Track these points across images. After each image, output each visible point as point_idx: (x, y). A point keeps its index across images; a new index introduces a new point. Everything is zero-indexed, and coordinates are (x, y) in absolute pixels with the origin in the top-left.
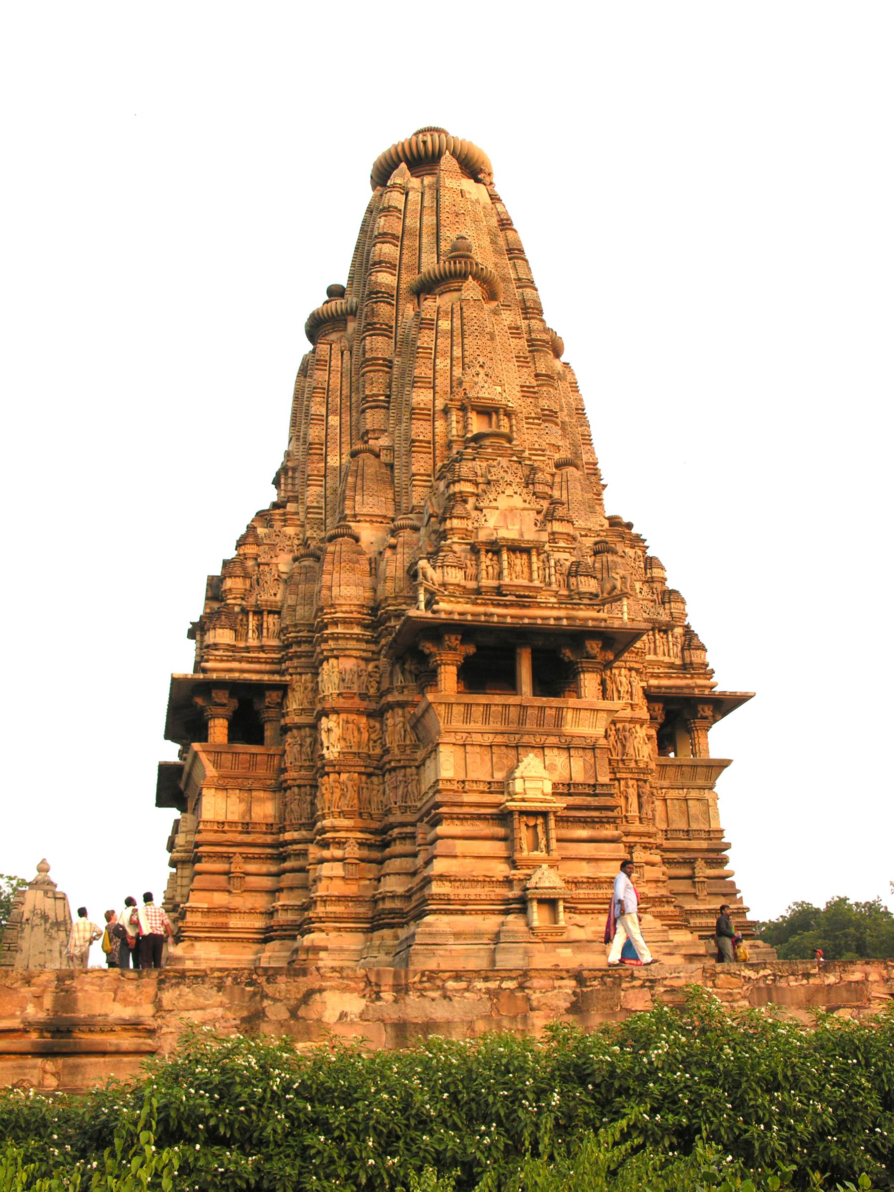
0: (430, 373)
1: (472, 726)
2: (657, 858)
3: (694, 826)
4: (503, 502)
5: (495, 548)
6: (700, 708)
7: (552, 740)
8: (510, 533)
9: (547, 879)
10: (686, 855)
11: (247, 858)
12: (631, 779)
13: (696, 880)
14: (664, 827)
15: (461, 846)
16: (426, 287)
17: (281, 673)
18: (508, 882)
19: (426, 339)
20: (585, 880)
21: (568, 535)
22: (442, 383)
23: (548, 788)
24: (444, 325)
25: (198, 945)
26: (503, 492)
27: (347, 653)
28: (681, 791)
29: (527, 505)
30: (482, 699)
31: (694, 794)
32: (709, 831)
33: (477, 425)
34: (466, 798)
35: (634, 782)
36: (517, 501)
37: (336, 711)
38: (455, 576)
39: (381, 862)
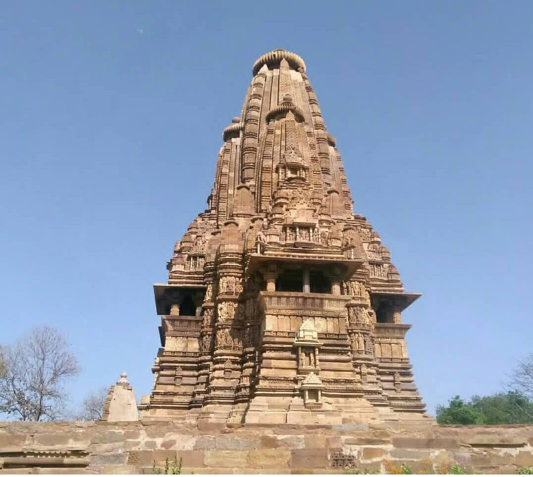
0: (271, 153)
2: (373, 371)
3: (395, 357)
4: (298, 207)
5: (293, 227)
7: (319, 313)
8: (302, 220)
9: (312, 380)
11: (184, 369)
13: (396, 382)
14: (380, 357)
15: (274, 363)
16: (271, 117)
17: (204, 284)
18: (295, 381)
19: (270, 138)
20: (333, 380)
22: (277, 157)
23: (315, 335)
24: (278, 132)
25: (158, 410)
27: (230, 274)
28: (388, 340)
29: (309, 208)
30: (286, 294)
31: (394, 341)
33: (289, 174)
34: (277, 340)
37: (226, 300)
38: (275, 239)
39: (241, 370)
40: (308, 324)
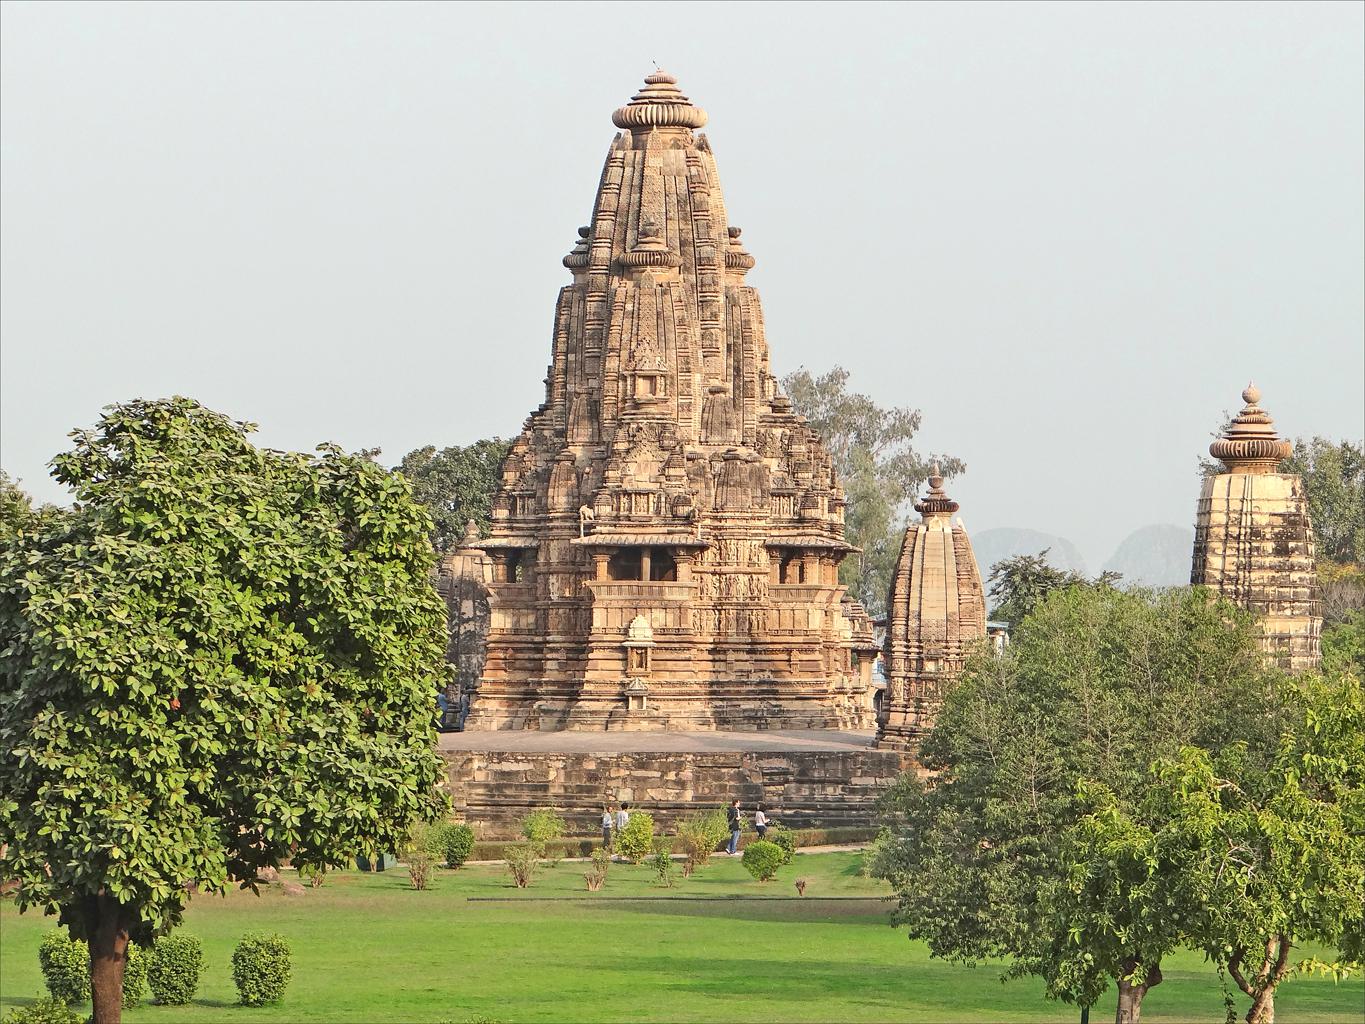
1: (612, 597)
3: (797, 627)
7: (657, 604)
10: (787, 646)
31: (799, 606)
34: (606, 638)
36: (649, 457)
37: (557, 573)
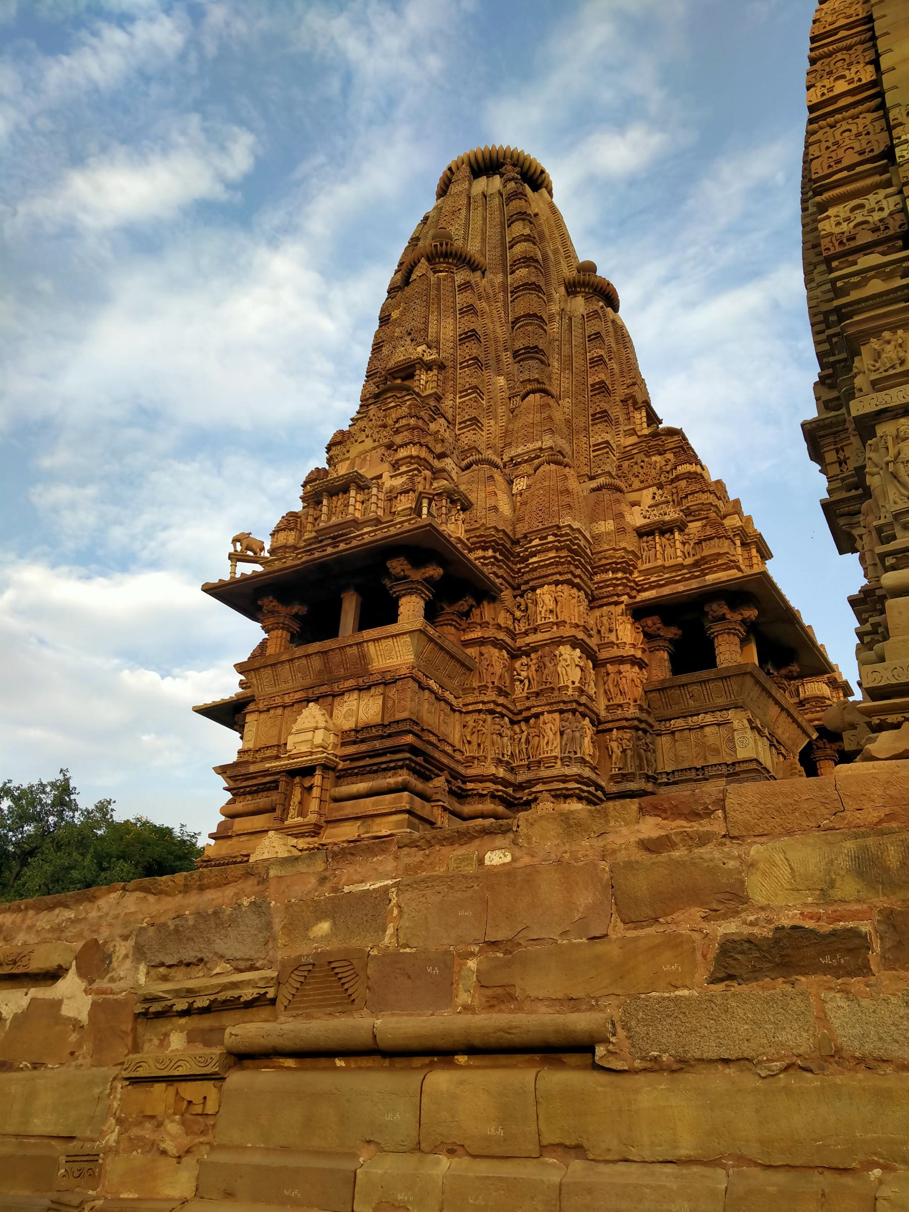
1: (284, 686)
3: (713, 761)
6: (706, 609)
12: (549, 712)
21: (411, 457)
26: (356, 441)
31: (709, 718)
32: (733, 764)
35: (556, 716)
40: (313, 714)
